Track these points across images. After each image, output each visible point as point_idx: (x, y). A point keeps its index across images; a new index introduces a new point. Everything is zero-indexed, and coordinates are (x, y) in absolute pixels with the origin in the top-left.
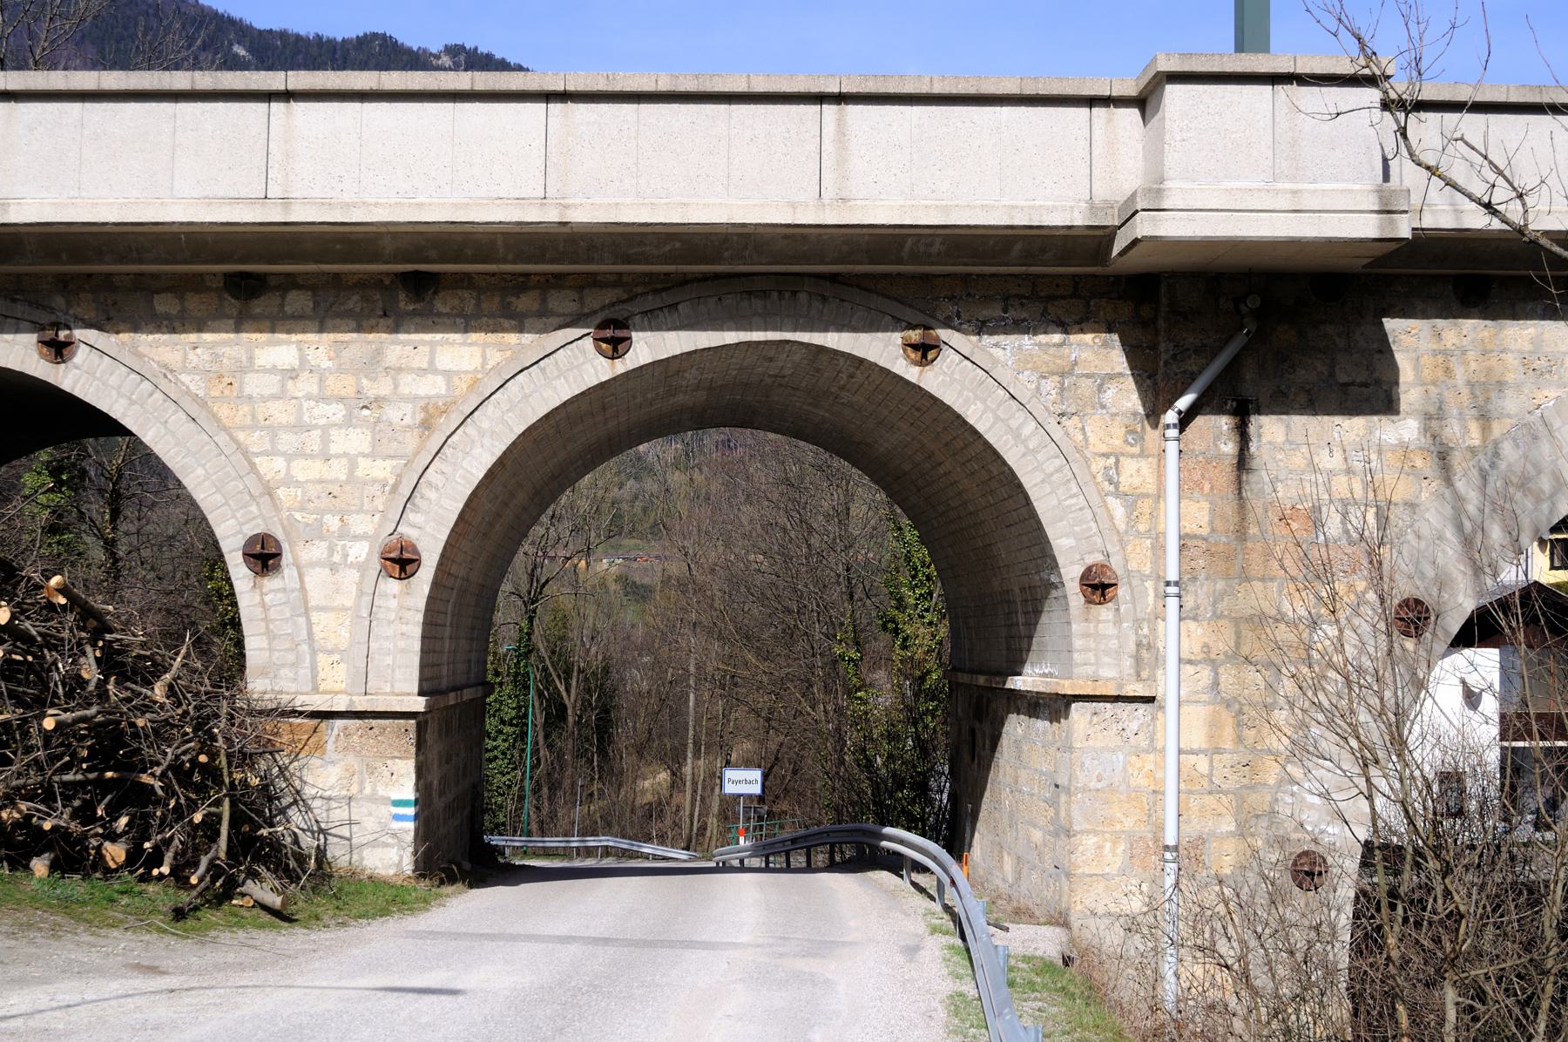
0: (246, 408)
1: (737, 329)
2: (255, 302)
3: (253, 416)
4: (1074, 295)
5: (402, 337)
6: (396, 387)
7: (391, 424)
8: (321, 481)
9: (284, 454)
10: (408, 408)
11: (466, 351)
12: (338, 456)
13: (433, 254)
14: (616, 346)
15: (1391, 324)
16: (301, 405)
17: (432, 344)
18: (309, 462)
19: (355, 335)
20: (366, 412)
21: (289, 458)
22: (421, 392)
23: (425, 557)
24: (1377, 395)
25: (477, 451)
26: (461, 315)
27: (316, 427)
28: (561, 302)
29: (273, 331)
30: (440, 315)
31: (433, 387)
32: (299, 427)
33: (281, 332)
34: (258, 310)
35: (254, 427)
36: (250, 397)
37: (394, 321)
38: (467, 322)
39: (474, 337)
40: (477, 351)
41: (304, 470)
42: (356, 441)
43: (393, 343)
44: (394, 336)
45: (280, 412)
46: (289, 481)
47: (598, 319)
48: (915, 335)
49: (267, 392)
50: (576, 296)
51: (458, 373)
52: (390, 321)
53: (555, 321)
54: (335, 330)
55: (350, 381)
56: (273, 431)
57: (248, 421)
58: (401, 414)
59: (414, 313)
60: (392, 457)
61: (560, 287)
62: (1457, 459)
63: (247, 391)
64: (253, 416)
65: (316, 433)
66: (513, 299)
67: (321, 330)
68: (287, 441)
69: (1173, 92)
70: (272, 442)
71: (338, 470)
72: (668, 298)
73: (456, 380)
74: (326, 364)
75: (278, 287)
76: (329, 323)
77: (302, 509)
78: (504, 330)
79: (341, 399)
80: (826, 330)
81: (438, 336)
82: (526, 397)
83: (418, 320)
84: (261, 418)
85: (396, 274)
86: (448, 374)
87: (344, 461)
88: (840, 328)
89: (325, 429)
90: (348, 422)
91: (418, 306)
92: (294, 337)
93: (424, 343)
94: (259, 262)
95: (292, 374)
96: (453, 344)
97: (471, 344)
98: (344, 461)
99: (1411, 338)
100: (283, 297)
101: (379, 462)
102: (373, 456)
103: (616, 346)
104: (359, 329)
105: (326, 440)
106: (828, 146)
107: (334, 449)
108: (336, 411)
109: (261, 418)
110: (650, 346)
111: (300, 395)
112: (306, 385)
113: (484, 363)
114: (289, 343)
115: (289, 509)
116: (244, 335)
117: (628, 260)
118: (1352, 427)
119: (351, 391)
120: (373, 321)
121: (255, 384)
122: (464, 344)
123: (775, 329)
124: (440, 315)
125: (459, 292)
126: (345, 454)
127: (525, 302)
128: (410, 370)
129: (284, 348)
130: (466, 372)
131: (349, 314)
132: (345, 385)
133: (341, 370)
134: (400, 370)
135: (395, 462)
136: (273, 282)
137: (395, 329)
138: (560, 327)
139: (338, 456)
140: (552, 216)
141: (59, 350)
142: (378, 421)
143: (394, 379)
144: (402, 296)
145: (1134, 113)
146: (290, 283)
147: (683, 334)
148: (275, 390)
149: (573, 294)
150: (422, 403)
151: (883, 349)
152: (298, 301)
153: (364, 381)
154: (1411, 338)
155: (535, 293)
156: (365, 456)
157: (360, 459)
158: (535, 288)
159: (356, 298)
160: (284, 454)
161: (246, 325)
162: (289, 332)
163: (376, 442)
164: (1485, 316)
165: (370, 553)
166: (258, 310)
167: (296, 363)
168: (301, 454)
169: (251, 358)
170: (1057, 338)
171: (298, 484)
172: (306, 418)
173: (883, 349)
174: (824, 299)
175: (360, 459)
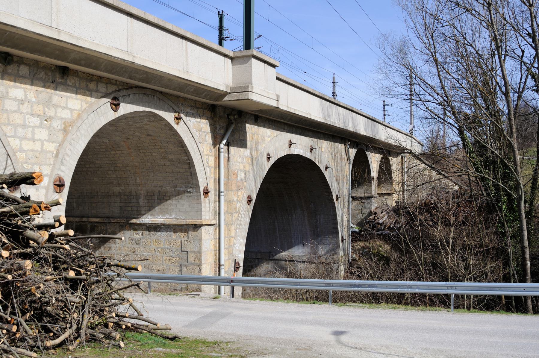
0: (5, 115)
1: (143, 106)
2: (9, 67)
3: (9, 120)
4: (202, 108)
5: (58, 92)
6: (56, 113)
7: (54, 128)
8: (32, 151)
9: (19, 138)
10: (59, 122)
11: (77, 101)
12: (38, 140)
13: (83, 62)
14: (115, 106)
15: (247, 125)
16: (25, 117)
17: (67, 97)
18: (28, 142)
19: (43, 89)
20: (46, 122)
21: (21, 139)
22: (64, 116)
23: (66, 184)
24: (243, 144)
25: (81, 142)
26: (75, 87)
27: (30, 127)
28: (102, 88)
29: (15, 82)
30: (69, 86)
31: (66, 114)
32: (25, 126)
33: (18, 83)
34: (10, 71)
35: (9, 124)
36: (7, 110)
37: (54, 84)
38: (77, 91)
39: (79, 96)
40: (79, 102)
41: (27, 145)
42: (42, 134)
43: (55, 94)
44: (55, 91)
45: (17, 118)
46: (21, 150)
47: (112, 96)
48: (176, 114)
49: (13, 109)
50: (105, 86)
51: (74, 110)
52: (54, 85)
53: (100, 95)
54: (36, 85)
55: (41, 108)
56: (15, 126)
57: (7, 122)
58: (57, 125)
59: (61, 83)
60: (54, 142)
61: (101, 82)
62: (254, 159)
63: (6, 107)
64: (9, 120)
65: (30, 129)
66: (89, 84)
67: (32, 84)
68: (20, 132)
69: (253, 60)
70: (15, 131)
71: (37, 146)
72: (129, 92)
73: (73, 112)
74: (34, 100)
75: (17, 62)
76: (35, 82)
77: (26, 163)
78: (87, 96)
79: (38, 116)
80: (160, 110)
81: (68, 94)
82: (93, 122)
83: (62, 86)
84: (11, 120)
85: (60, 66)
86: (71, 110)
87: (39, 142)
88: (163, 110)
89: (34, 127)
90: (41, 126)
91: (62, 81)
92: (23, 86)
93: (65, 96)
94: (22, 49)
95: (21, 102)
96: (72, 98)
97: (78, 99)
98: (39, 142)
99: (252, 130)
100: (19, 67)
101: (51, 144)
102: (49, 141)
103: (115, 106)
104: (44, 87)
105: (33, 133)
106: (184, 53)
107: (36, 137)
108: (36, 121)
109: (11, 120)
110: (126, 108)
111: (24, 112)
112: (25, 108)
113: (81, 107)
114: (21, 88)
115: (22, 162)
116: (5, 81)
117: (131, 78)
118: (242, 150)
119: (41, 113)
120: (49, 84)
121: (10, 105)
122: (76, 99)
123: (150, 108)
124: (69, 86)
125: (74, 77)
126: (40, 140)
127: (92, 85)
128: (60, 107)
129: (19, 90)
130: (76, 110)
131: (40, 79)
132: (39, 109)
133: (38, 103)
134: (57, 106)
135: (55, 144)
136: (15, 59)
137: (55, 89)
138: (101, 97)
139: (38, 140)
140: (131, 59)
141: (178, 119)
142: (50, 127)
143: (55, 109)
144: (57, 76)
145: (230, 61)
146: (21, 61)
147: (131, 106)
148: (16, 108)
149: (104, 85)
150: (64, 121)
151: (169, 117)
152: (24, 70)
153: (46, 109)
154: (252, 130)
155: (95, 82)
156: (46, 141)
157: (45, 142)
158: (95, 81)
159: (43, 73)
160: (19, 138)
161: (5, 77)
162: (21, 83)
163: (50, 135)
164: (258, 126)
165: (49, 183)
166: (10, 71)
167: (23, 97)
168: (25, 138)
169: (7, 93)
170: (199, 120)
171: (25, 151)
172: (27, 122)
173: (169, 117)
174: (160, 99)
175: (45, 142)
